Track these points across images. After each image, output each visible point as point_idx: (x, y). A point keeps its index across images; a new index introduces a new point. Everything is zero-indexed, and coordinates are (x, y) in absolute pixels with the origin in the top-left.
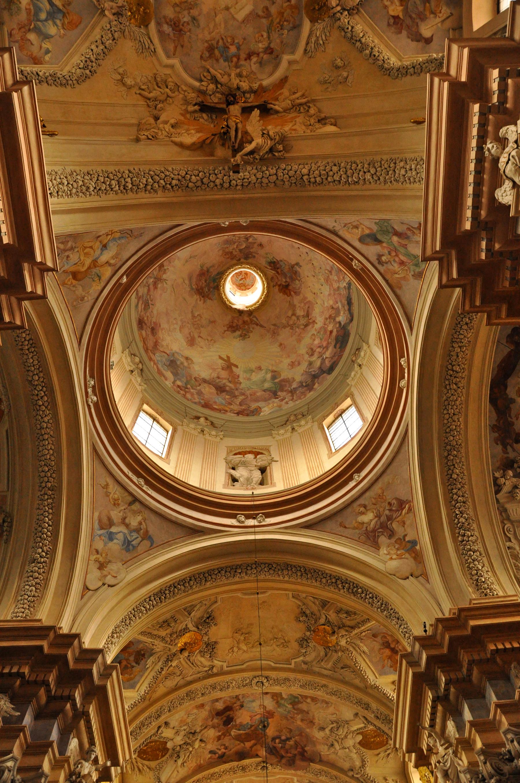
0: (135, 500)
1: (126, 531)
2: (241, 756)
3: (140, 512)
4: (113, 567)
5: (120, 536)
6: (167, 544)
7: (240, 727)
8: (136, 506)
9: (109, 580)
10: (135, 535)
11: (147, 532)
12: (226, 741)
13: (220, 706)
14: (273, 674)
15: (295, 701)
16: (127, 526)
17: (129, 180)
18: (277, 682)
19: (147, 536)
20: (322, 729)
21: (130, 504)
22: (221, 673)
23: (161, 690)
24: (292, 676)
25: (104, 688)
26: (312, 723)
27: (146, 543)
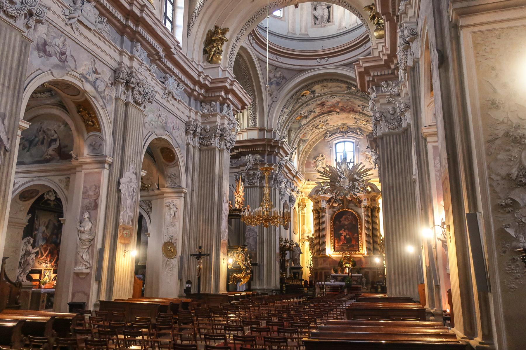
0: (277, 67)
1: (275, 79)
2: (330, 112)
3: (279, 71)
4: (274, 94)
5: (275, 82)
6: (292, 78)
7: (328, 105)
8: (278, 69)
9: (274, 99)
10: (279, 79)
11: (283, 76)
12: (323, 109)
13: (319, 102)
14: (338, 95)
15: (348, 100)
16: (276, 77)
17: (255, 19)
18: (340, 96)
19: (284, 78)
20: (359, 106)
21: (276, 69)
22: (318, 96)
23: (297, 107)
24: (345, 95)
25: (283, 147)
26: (355, 104)
27: (284, 80)
